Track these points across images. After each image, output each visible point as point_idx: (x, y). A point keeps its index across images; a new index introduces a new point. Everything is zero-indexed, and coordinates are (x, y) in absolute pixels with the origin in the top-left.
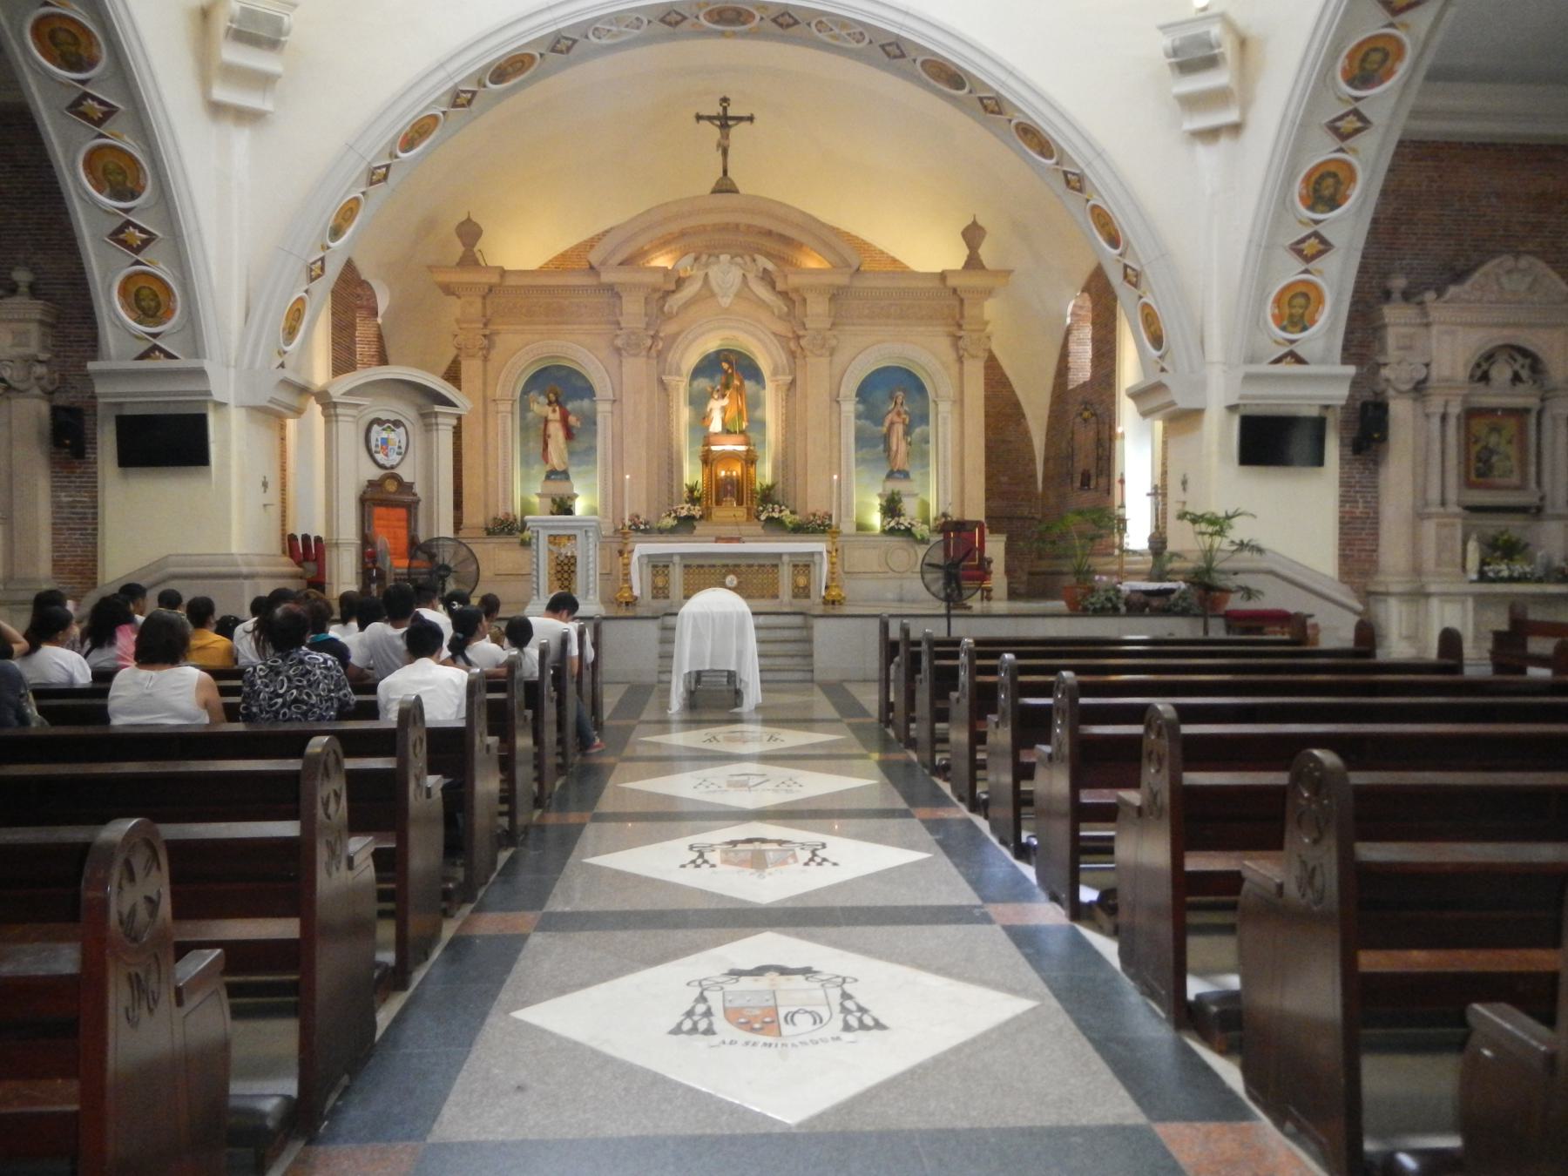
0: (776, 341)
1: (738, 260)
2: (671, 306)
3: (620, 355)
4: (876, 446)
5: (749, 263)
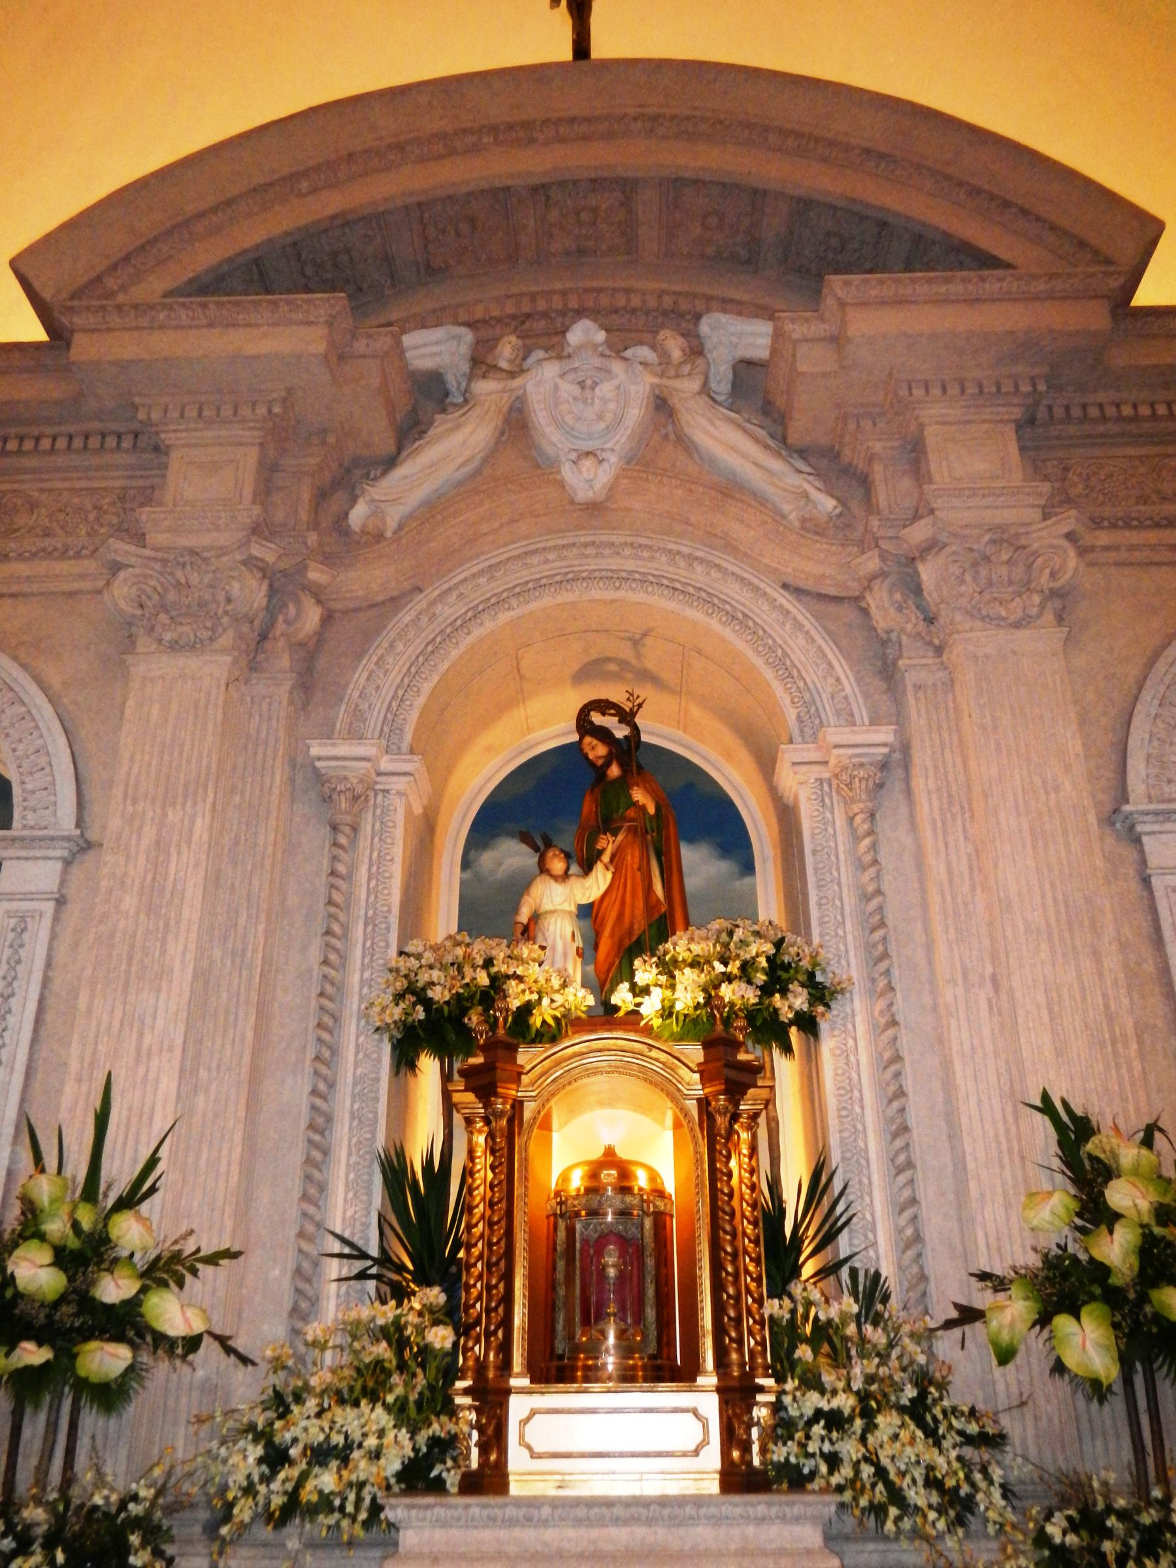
1: (644, 352)
2: (377, 512)
5: (676, 354)
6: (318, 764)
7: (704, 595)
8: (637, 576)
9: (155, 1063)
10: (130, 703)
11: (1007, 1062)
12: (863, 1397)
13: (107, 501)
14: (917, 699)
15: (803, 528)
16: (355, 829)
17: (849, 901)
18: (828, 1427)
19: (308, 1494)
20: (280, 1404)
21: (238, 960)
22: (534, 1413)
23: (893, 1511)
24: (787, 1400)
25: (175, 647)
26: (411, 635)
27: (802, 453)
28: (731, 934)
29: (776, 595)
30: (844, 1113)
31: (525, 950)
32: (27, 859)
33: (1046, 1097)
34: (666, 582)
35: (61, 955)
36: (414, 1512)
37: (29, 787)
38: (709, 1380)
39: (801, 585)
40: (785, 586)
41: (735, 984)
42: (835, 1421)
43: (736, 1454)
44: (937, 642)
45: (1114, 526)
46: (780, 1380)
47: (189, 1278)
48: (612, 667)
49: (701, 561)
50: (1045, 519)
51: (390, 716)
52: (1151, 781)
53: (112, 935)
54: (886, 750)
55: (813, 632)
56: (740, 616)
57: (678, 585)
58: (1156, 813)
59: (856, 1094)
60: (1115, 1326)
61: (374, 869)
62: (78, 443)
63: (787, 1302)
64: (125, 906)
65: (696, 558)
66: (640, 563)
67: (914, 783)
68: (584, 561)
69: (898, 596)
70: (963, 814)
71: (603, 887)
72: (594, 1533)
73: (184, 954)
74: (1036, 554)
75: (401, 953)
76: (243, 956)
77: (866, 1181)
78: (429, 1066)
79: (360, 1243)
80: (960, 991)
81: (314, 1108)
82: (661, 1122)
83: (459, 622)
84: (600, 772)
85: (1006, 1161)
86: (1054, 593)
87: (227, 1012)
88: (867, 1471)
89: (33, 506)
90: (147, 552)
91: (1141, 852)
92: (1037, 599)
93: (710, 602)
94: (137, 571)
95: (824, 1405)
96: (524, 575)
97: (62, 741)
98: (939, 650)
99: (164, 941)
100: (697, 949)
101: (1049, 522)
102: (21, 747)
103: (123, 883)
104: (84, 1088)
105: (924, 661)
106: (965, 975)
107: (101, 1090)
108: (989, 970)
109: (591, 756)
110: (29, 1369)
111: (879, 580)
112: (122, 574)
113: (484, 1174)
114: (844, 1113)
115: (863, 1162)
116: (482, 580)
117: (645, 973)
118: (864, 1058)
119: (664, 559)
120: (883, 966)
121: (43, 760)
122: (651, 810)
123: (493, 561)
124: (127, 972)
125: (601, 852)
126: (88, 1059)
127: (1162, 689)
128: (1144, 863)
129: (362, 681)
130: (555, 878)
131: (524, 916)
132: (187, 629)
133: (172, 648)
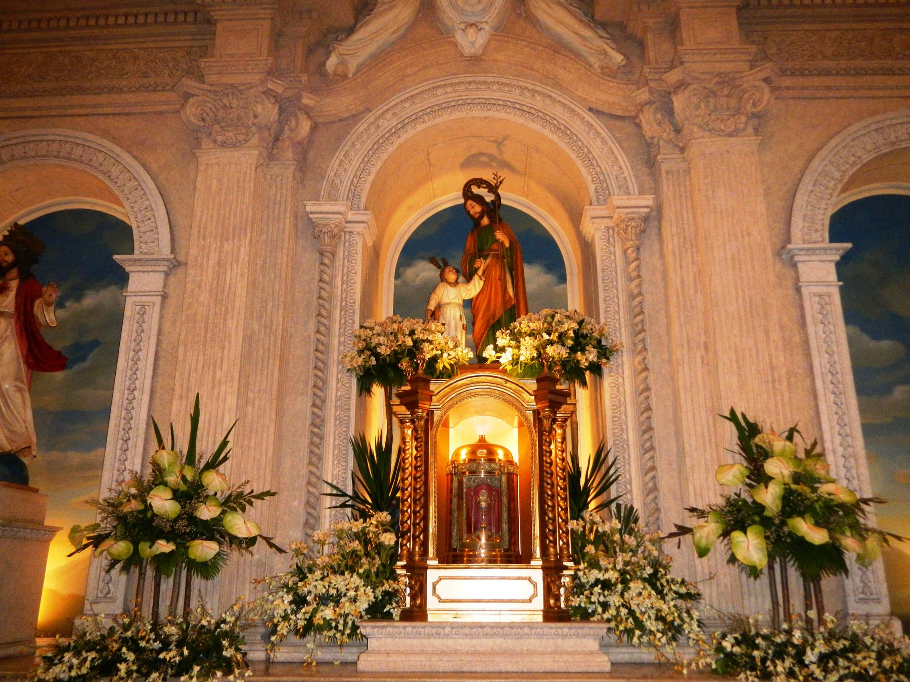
0: (604, 133)
2: (343, 62)
3: (198, 143)
4: (889, 390)
6: (311, 216)
7: (541, 114)
8: (501, 102)
9: (223, 387)
10: (199, 179)
11: (711, 392)
12: (623, 573)
13: (180, 54)
14: (668, 179)
15: (602, 73)
16: (334, 254)
17: (623, 299)
18: (603, 589)
19: (318, 620)
20: (301, 573)
21: (268, 330)
22: (440, 579)
23: (638, 633)
24: (580, 574)
25: (224, 145)
26: (365, 138)
27: (604, 25)
28: (553, 317)
29: (585, 115)
30: (616, 419)
31: (433, 326)
32: (144, 272)
33: (732, 412)
34: (518, 106)
35: (166, 328)
36: (376, 630)
37: (142, 229)
38: (537, 562)
39: (600, 109)
40: (590, 110)
41: (555, 347)
42: (606, 585)
43: (552, 602)
44: (681, 145)
45: (793, 74)
46: (577, 563)
47: (248, 506)
48: (484, 159)
49: (540, 93)
50: (751, 69)
51: (353, 188)
52: (806, 230)
53: (195, 315)
54: (647, 210)
55: (607, 138)
56: (563, 127)
57: (525, 108)
58: (808, 250)
59: (623, 408)
60: (767, 538)
61: (345, 278)
62: (161, 18)
63: (581, 522)
64: (202, 299)
65: (537, 92)
66: (504, 94)
67: (663, 231)
68: (468, 93)
69: (659, 116)
70: (692, 248)
71: (478, 290)
72: (474, 642)
73: (237, 327)
74: (745, 91)
75: (361, 327)
76: (271, 328)
77: (627, 457)
78: (378, 391)
79: (342, 488)
80: (685, 351)
81: (314, 413)
82: (510, 423)
83: (393, 130)
84: (477, 222)
85: (707, 446)
86: (754, 115)
87: (263, 361)
88: (624, 611)
89: (136, 58)
90: (205, 86)
91: (797, 272)
92: (743, 119)
93: (547, 120)
94: (200, 98)
95: (601, 576)
96: (434, 101)
97: (161, 202)
98: (682, 150)
99: (225, 320)
100: (532, 325)
101: (754, 71)
102: (136, 205)
103: (200, 286)
104: (184, 402)
105: (672, 156)
106: (689, 342)
107: (193, 403)
108: (703, 339)
109: (471, 212)
110: (163, 554)
111: (648, 106)
112: (191, 100)
113: (411, 451)
114: (616, 419)
115: (625, 446)
116: (407, 105)
117: (503, 340)
118: (628, 388)
119: (517, 92)
120: (641, 336)
121: (149, 214)
122: (507, 245)
123: (413, 93)
124: (205, 337)
125: (477, 269)
126: (185, 386)
127: (816, 174)
128: (797, 279)
129: (336, 166)
130: (450, 284)
131: (432, 306)
132: (231, 134)
133: (223, 146)
